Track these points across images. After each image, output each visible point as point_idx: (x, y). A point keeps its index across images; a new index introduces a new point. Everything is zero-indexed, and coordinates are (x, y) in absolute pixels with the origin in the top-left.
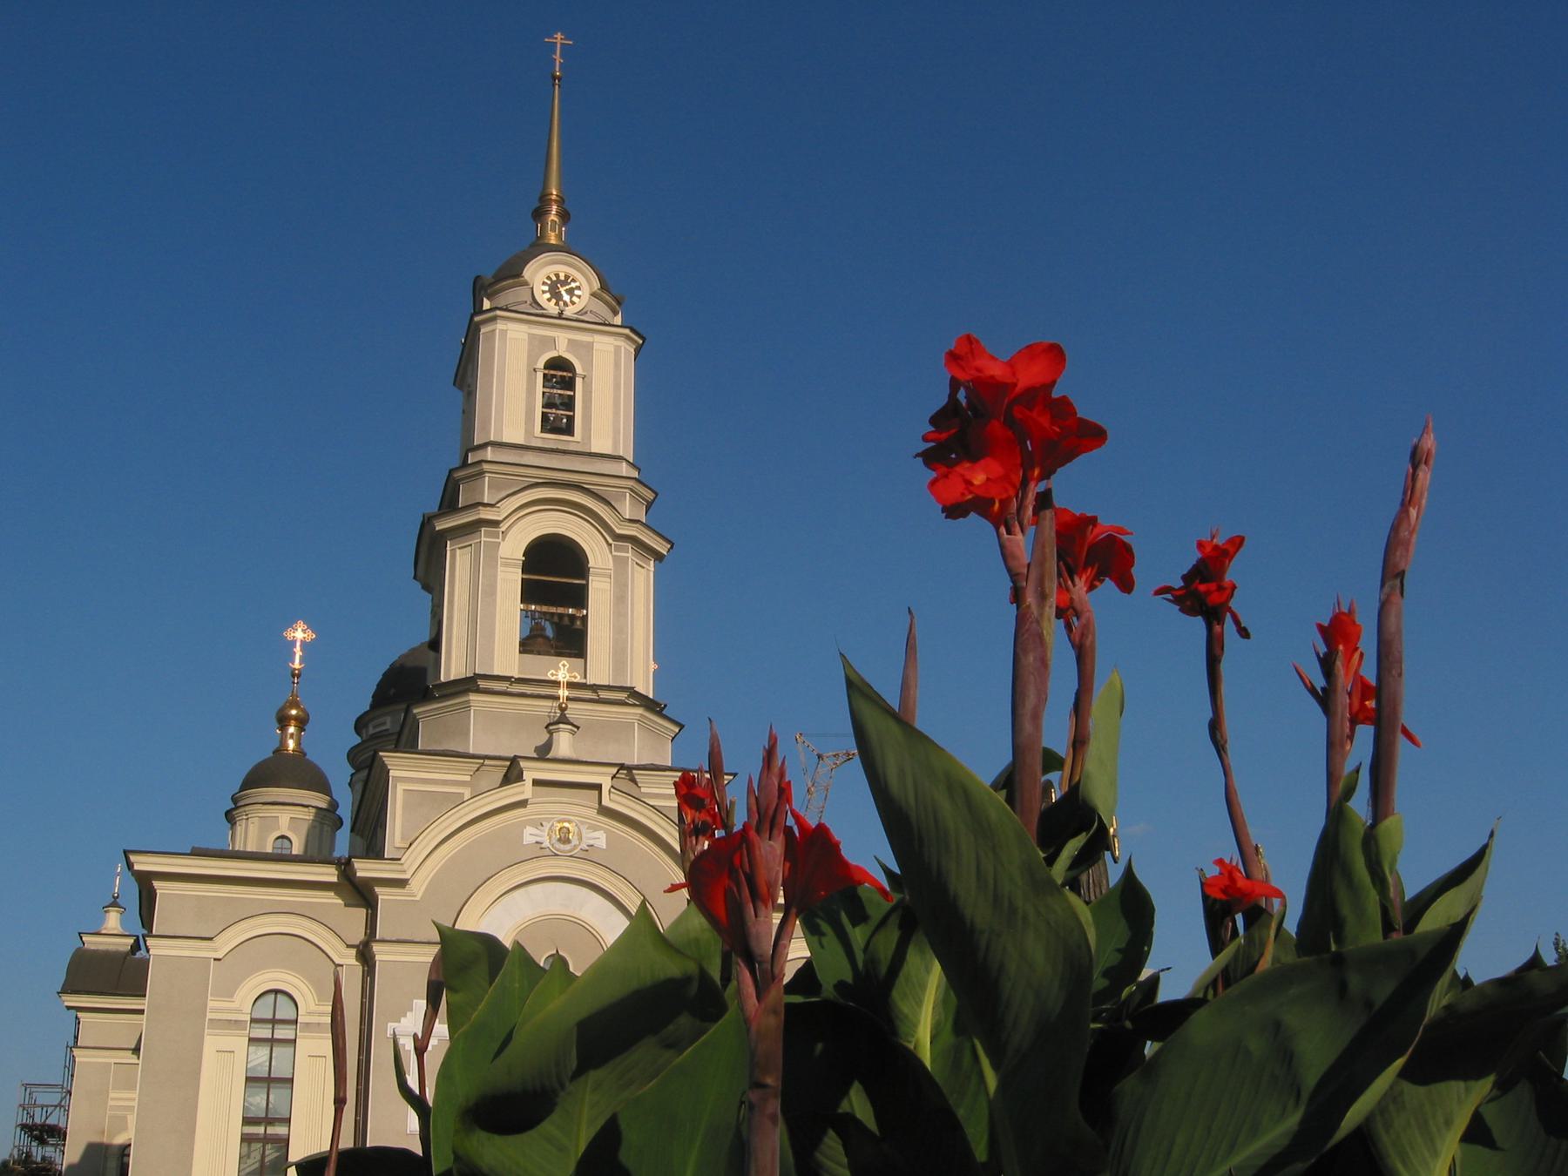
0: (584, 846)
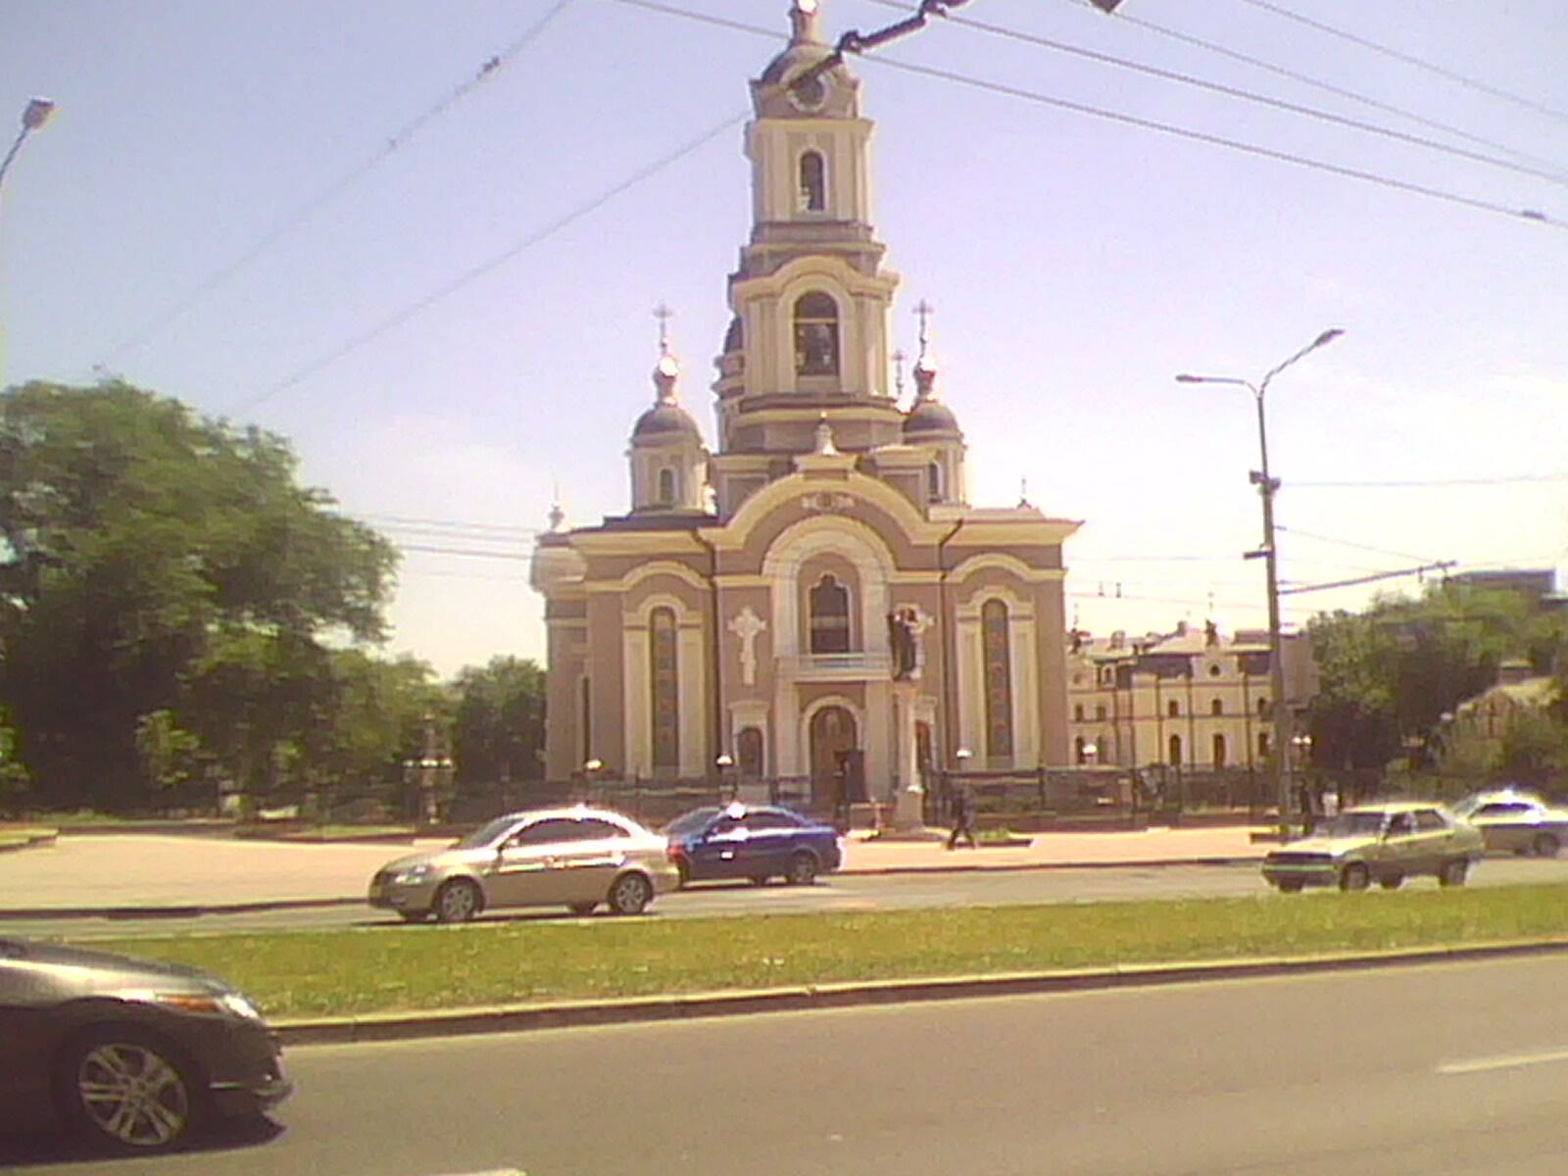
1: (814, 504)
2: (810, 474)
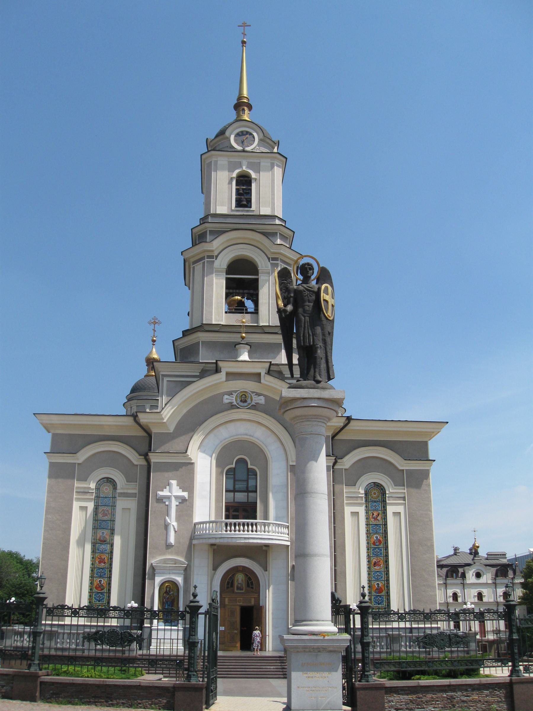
0: (253, 403)
1: (233, 399)
2: (230, 376)
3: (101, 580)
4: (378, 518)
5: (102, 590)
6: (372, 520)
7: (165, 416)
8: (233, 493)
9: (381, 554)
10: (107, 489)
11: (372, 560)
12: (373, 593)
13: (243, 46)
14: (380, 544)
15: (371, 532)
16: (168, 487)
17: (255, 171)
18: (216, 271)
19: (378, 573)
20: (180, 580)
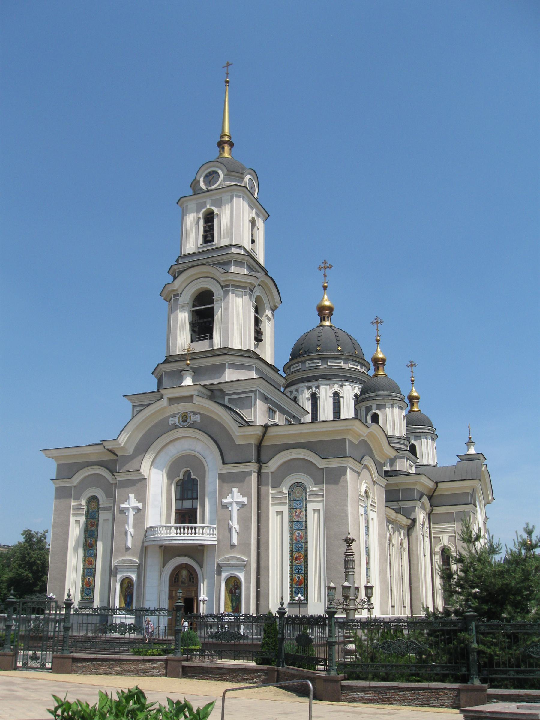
1: (175, 420)
3: (89, 578)
4: (300, 516)
5: (90, 586)
6: (295, 518)
7: (122, 442)
8: (191, 501)
9: (302, 549)
10: (298, 492)
11: (294, 554)
12: (294, 585)
13: (226, 85)
14: (302, 539)
15: (294, 528)
16: (230, 494)
17: (217, 207)
18: (181, 307)
19: (299, 567)
20: (134, 576)
